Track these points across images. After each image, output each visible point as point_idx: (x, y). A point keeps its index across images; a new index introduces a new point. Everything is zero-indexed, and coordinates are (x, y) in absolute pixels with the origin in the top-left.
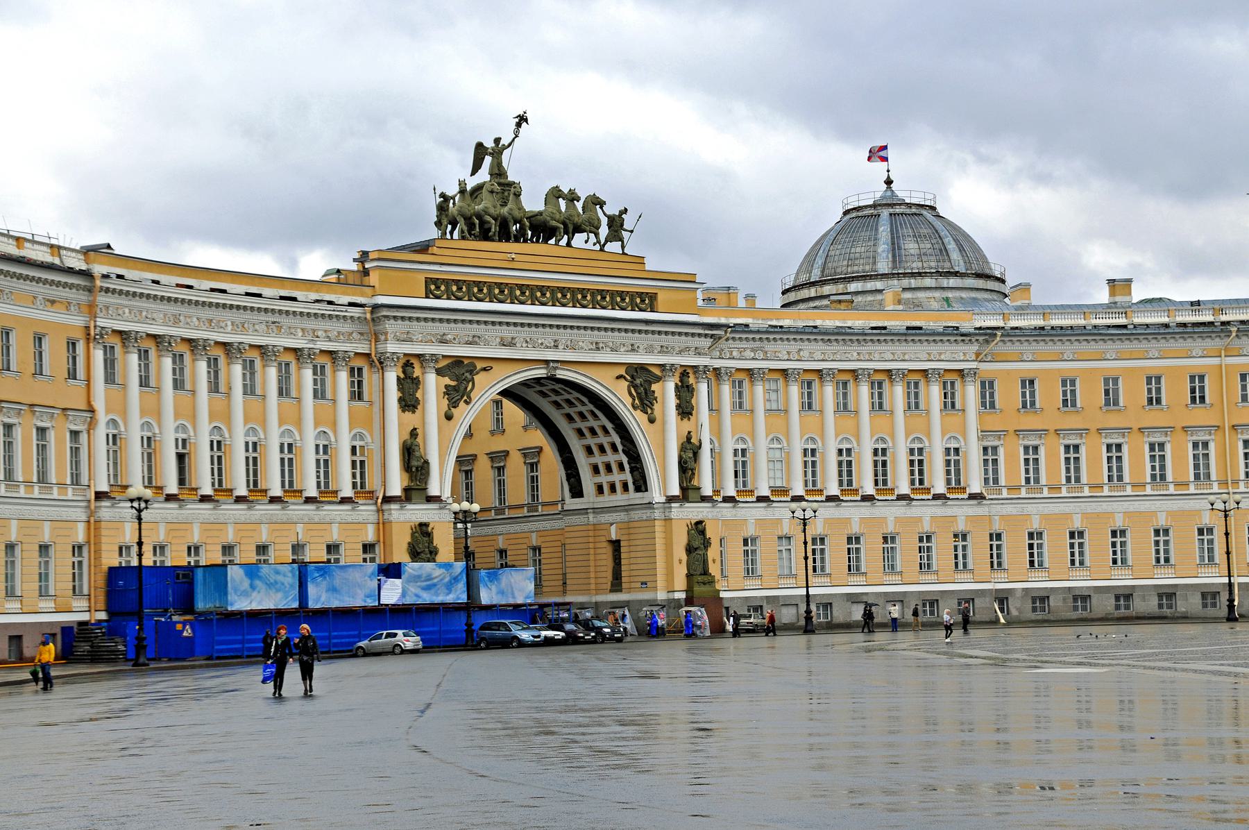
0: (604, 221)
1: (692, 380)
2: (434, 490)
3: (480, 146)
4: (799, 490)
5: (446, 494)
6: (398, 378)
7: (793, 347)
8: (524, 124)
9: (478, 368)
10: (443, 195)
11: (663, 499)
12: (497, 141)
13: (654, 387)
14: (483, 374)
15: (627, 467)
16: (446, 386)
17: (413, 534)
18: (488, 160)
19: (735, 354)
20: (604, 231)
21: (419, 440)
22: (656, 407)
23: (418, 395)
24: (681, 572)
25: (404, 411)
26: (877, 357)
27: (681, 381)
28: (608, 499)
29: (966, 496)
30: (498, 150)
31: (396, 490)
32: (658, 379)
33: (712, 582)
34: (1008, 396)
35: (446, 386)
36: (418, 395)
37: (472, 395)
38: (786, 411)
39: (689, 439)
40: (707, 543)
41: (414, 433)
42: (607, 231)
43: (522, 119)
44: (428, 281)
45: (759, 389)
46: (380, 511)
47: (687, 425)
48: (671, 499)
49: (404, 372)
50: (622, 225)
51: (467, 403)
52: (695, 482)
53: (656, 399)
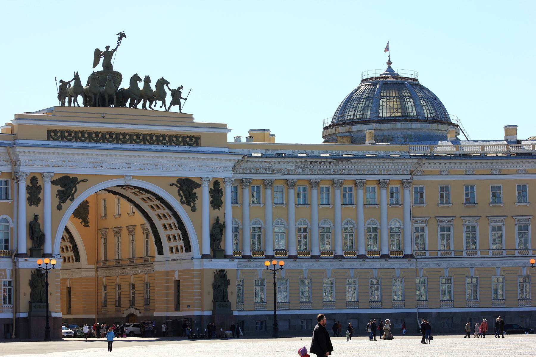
0: (169, 93)
1: (221, 187)
2: (48, 250)
6: (28, 188)
8: (124, 38)
9: (79, 180)
10: (61, 81)
11: (200, 256)
13: (195, 191)
14: (82, 183)
15: (181, 237)
16: (58, 191)
17: (32, 275)
18: (102, 59)
19: (253, 171)
20: (169, 99)
21: (39, 221)
22: (197, 202)
23: (40, 196)
24: (209, 299)
25: (31, 205)
26: (346, 172)
27: (214, 187)
28: (175, 256)
29: (402, 256)
30: (108, 54)
31: (23, 250)
32: (198, 186)
33: (228, 306)
34: (432, 196)
35: (58, 191)
37: (75, 196)
38: (287, 204)
39: (217, 220)
40: (227, 283)
41: (36, 217)
42: (171, 98)
43: (122, 36)
44: (49, 132)
45: (269, 192)
46: (15, 263)
47: (217, 213)
48: (204, 257)
49: (31, 183)
50: (180, 95)
51: (72, 200)
52: (222, 247)
53: (197, 197)
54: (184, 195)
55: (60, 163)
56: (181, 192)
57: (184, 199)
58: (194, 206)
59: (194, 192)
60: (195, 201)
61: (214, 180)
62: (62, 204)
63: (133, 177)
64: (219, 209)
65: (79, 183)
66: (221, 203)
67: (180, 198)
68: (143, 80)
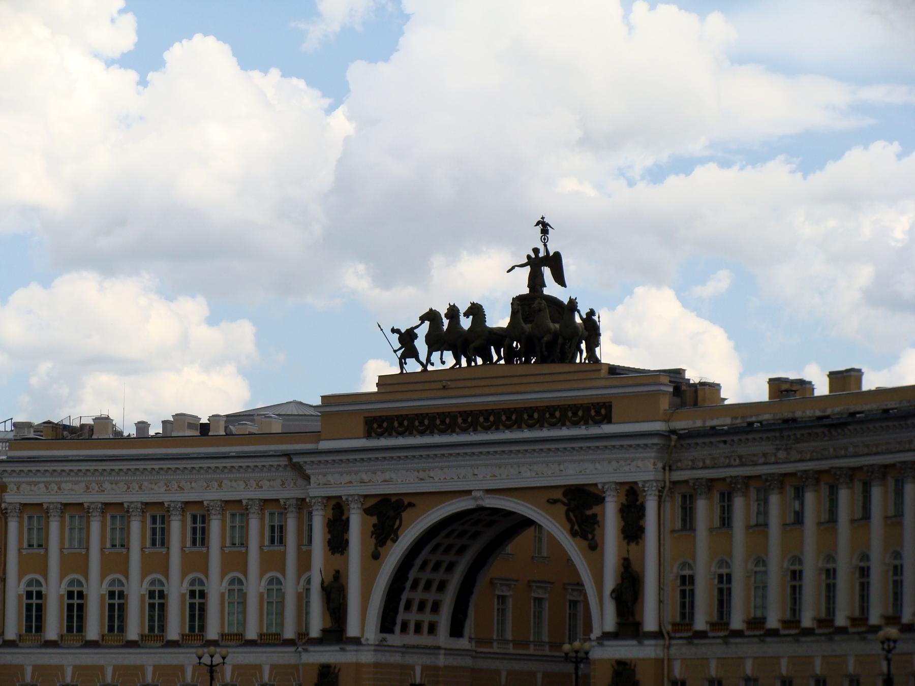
1: (640, 500)
2: (353, 630)
3: (529, 257)
4: (773, 622)
5: (371, 634)
7: (767, 447)
9: (406, 503)
10: (394, 331)
12: (536, 251)
13: (596, 510)
14: (409, 510)
16: (374, 526)
25: (333, 553)
32: (600, 500)
35: (374, 526)
36: (329, 536)
43: (545, 227)
51: (394, 541)
53: (597, 523)
54: (576, 517)
55: (365, 477)
56: (571, 514)
57: (576, 527)
58: (593, 538)
59: (589, 512)
60: (594, 530)
61: (627, 487)
62: (379, 549)
63: (488, 491)
64: (637, 543)
65: (405, 510)
66: (642, 530)
67: (568, 526)
68: (462, 315)
